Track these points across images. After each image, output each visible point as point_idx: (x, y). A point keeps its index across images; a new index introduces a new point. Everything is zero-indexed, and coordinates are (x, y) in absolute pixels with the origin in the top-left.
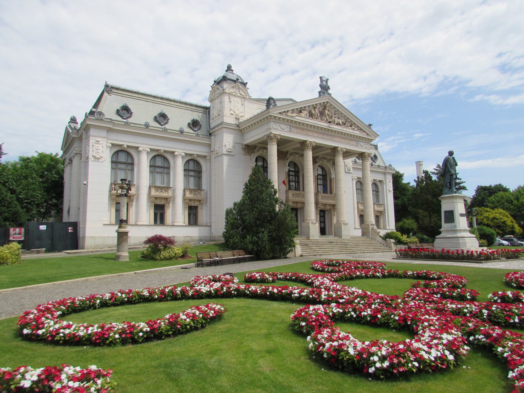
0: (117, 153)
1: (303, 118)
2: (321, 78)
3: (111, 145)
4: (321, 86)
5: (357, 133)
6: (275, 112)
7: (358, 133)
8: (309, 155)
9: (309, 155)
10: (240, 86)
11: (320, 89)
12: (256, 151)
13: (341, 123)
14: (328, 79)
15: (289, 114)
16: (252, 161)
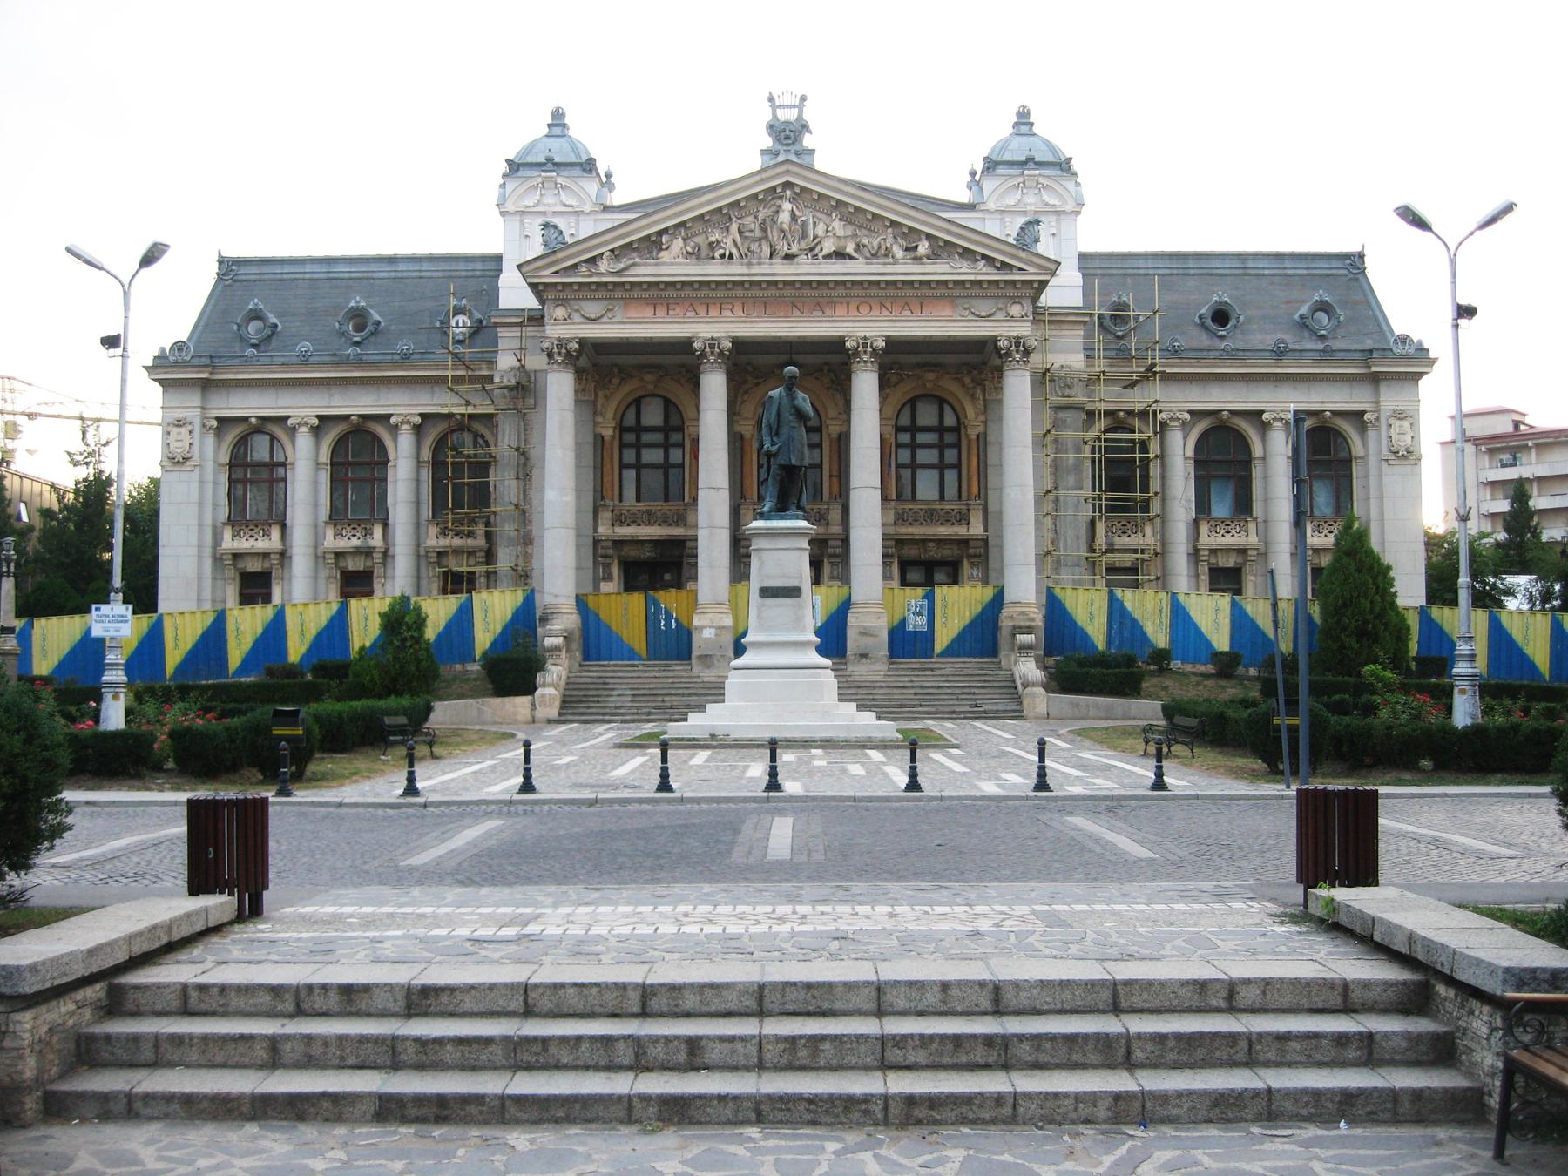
0: (242, 442)
1: (672, 265)
2: (771, 99)
3: (215, 423)
4: (771, 128)
5: (940, 270)
6: (547, 272)
7: (946, 268)
8: (714, 386)
9: (714, 386)
10: (559, 180)
11: (768, 142)
12: (616, 381)
13: (850, 249)
14: (803, 98)
15: (603, 266)
16: (600, 419)
